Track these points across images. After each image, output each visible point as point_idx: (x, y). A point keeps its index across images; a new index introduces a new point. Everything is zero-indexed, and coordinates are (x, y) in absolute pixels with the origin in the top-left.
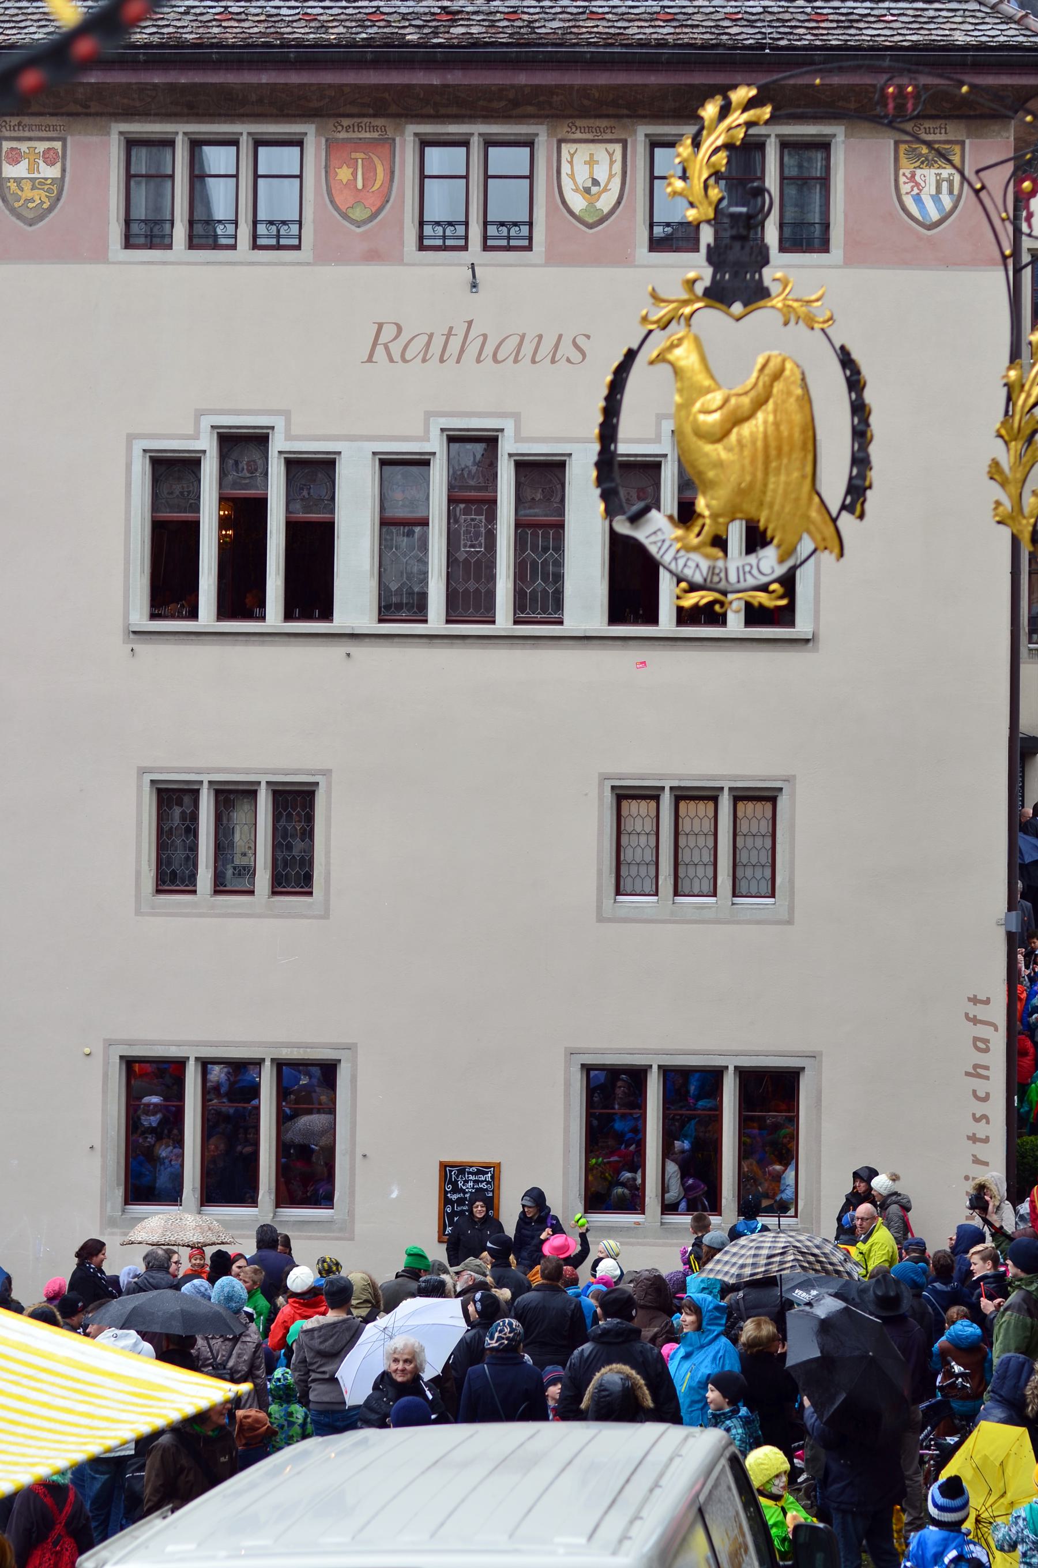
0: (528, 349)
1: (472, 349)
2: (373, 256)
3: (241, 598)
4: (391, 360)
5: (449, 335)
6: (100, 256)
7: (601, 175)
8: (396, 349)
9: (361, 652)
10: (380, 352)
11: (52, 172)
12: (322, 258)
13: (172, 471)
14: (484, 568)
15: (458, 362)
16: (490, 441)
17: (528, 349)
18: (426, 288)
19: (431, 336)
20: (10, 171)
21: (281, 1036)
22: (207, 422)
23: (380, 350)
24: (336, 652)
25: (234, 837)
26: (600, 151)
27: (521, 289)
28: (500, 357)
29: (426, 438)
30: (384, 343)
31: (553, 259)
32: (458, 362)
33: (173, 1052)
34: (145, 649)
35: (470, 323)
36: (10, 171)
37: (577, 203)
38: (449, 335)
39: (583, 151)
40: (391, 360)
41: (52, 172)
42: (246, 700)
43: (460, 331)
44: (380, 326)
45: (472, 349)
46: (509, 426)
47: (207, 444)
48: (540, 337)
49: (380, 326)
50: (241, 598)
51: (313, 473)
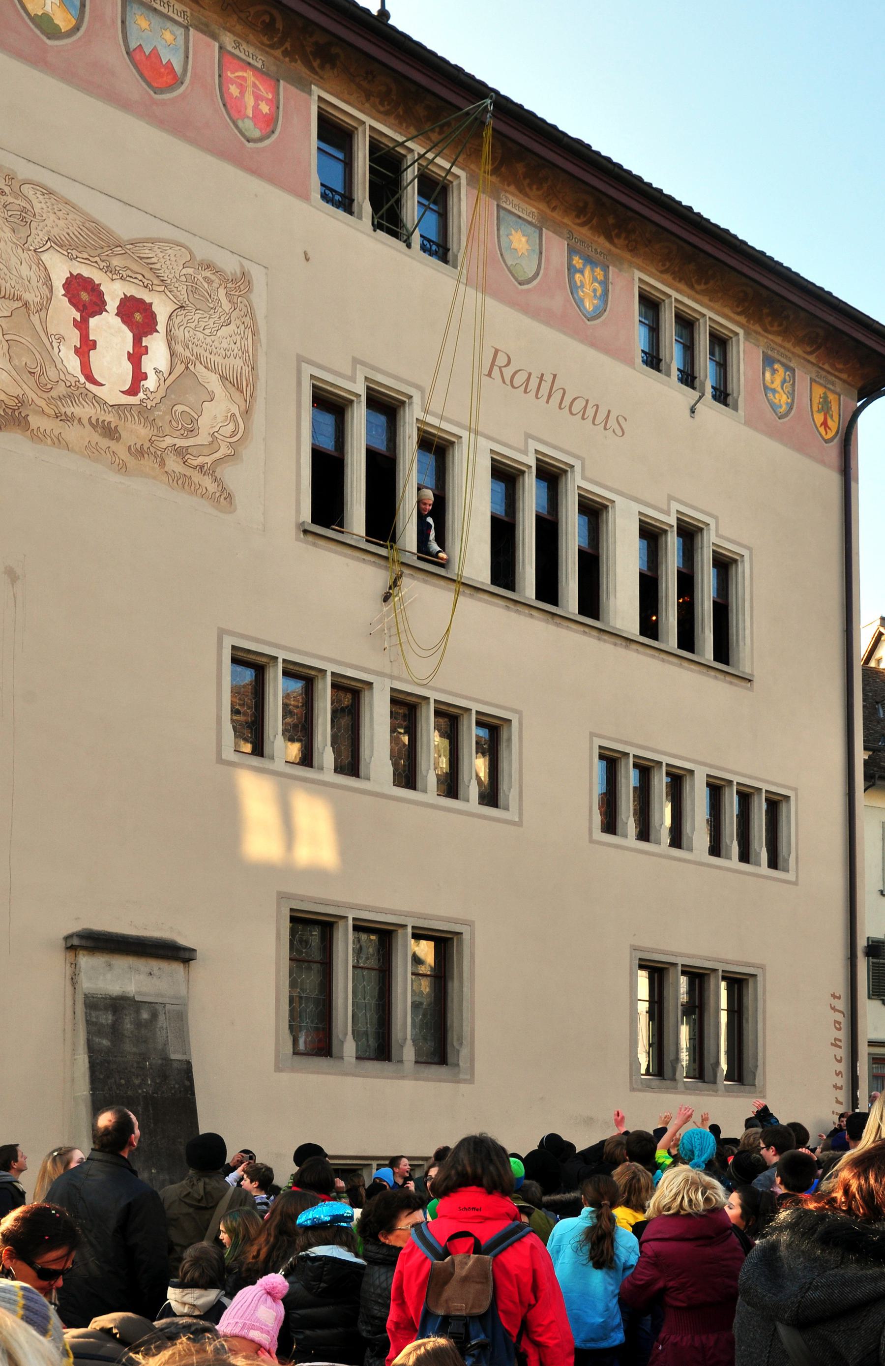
0: (590, 412)
4: (504, 382)
5: (541, 378)
8: (508, 372)
10: (496, 372)
15: (547, 402)
17: (590, 412)
19: (530, 374)
23: (496, 370)
28: (574, 411)
29: (525, 452)
32: (547, 402)
35: (555, 376)
38: (541, 378)
40: (504, 382)
43: (548, 378)
44: (497, 351)
48: (597, 406)
49: (497, 351)
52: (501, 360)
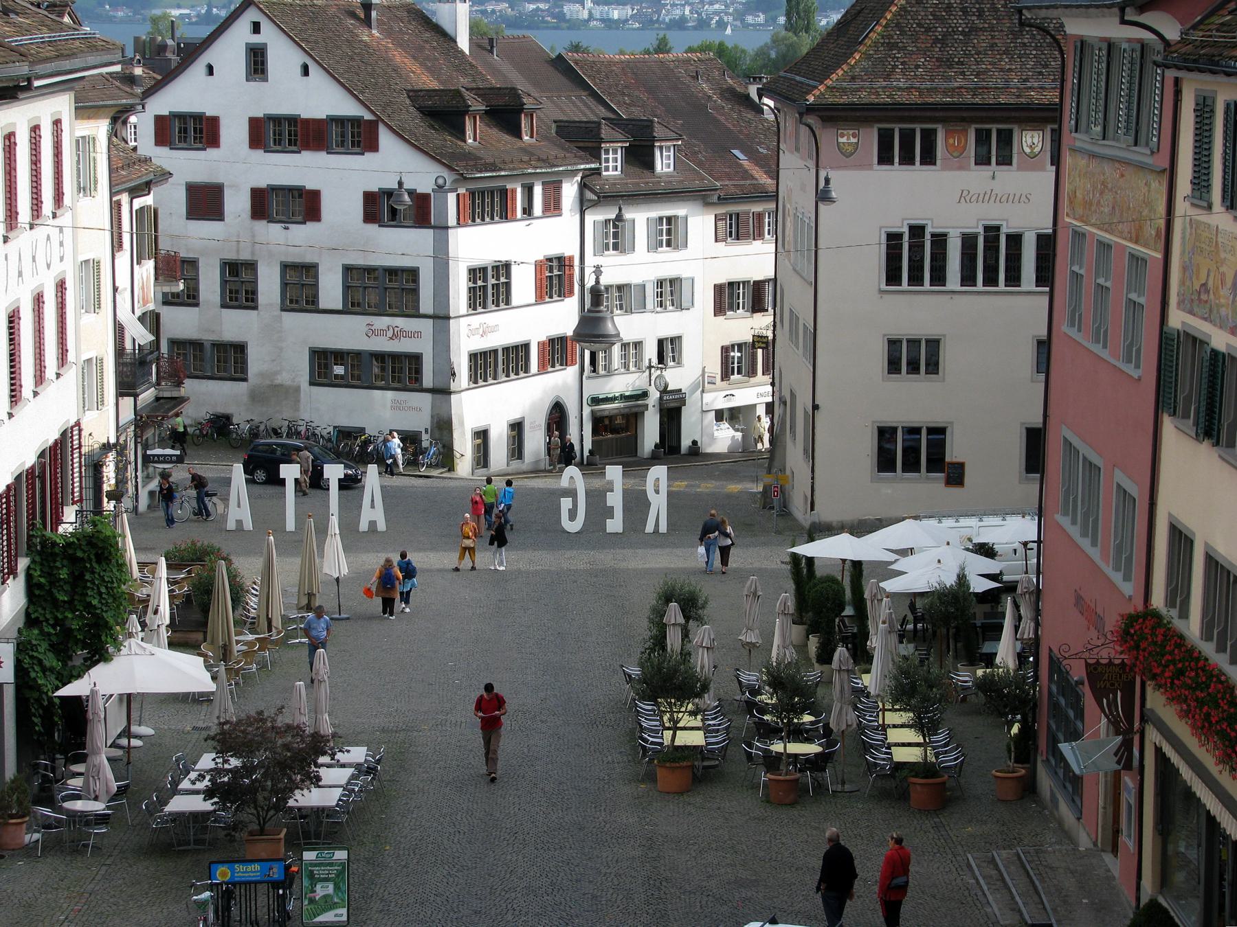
0: (1011, 198)
1: (993, 199)
2: (961, 168)
3: (916, 279)
6: (870, 167)
7: (1035, 141)
9: (956, 297)
11: (855, 140)
12: (944, 169)
13: (893, 239)
14: (996, 270)
16: (998, 228)
17: (1011, 198)
18: (977, 178)
20: (841, 140)
21: (929, 419)
22: (906, 223)
24: (948, 297)
25: (913, 357)
26: (1035, 134)
27: (1008, 179)
30: (964, 197)
31: (1019, 169)
33: (894, 425)
34: (886, 297)
36: (841, 140)
37: (1027, 150)
39: (1029, 134)
41: (854, 140)
42: (918, 312)
45: (993, 199)
46: (1004, 224)
47: (906, 230)
50: (916, 279)
51: (940, 240)
52: (965, 193)
